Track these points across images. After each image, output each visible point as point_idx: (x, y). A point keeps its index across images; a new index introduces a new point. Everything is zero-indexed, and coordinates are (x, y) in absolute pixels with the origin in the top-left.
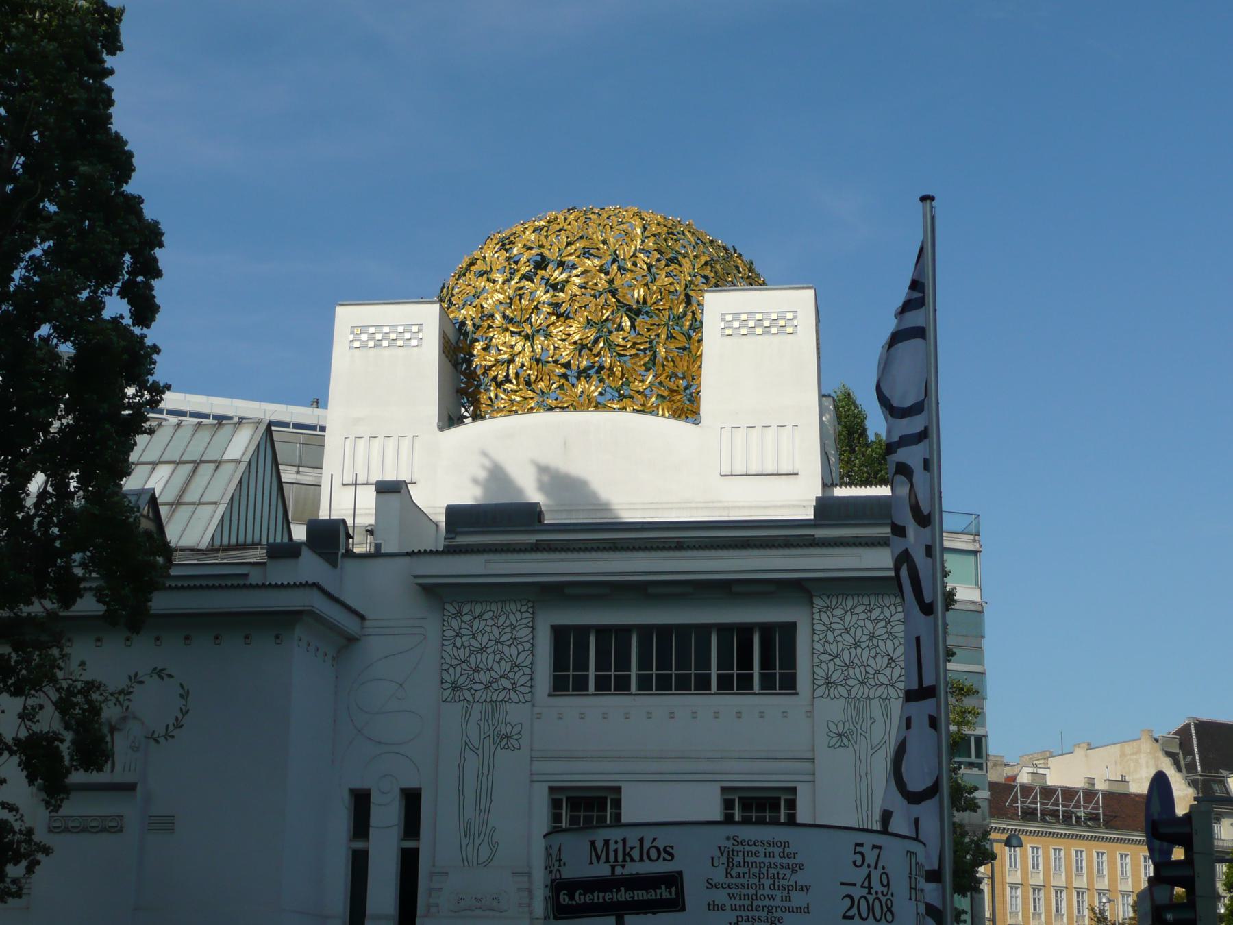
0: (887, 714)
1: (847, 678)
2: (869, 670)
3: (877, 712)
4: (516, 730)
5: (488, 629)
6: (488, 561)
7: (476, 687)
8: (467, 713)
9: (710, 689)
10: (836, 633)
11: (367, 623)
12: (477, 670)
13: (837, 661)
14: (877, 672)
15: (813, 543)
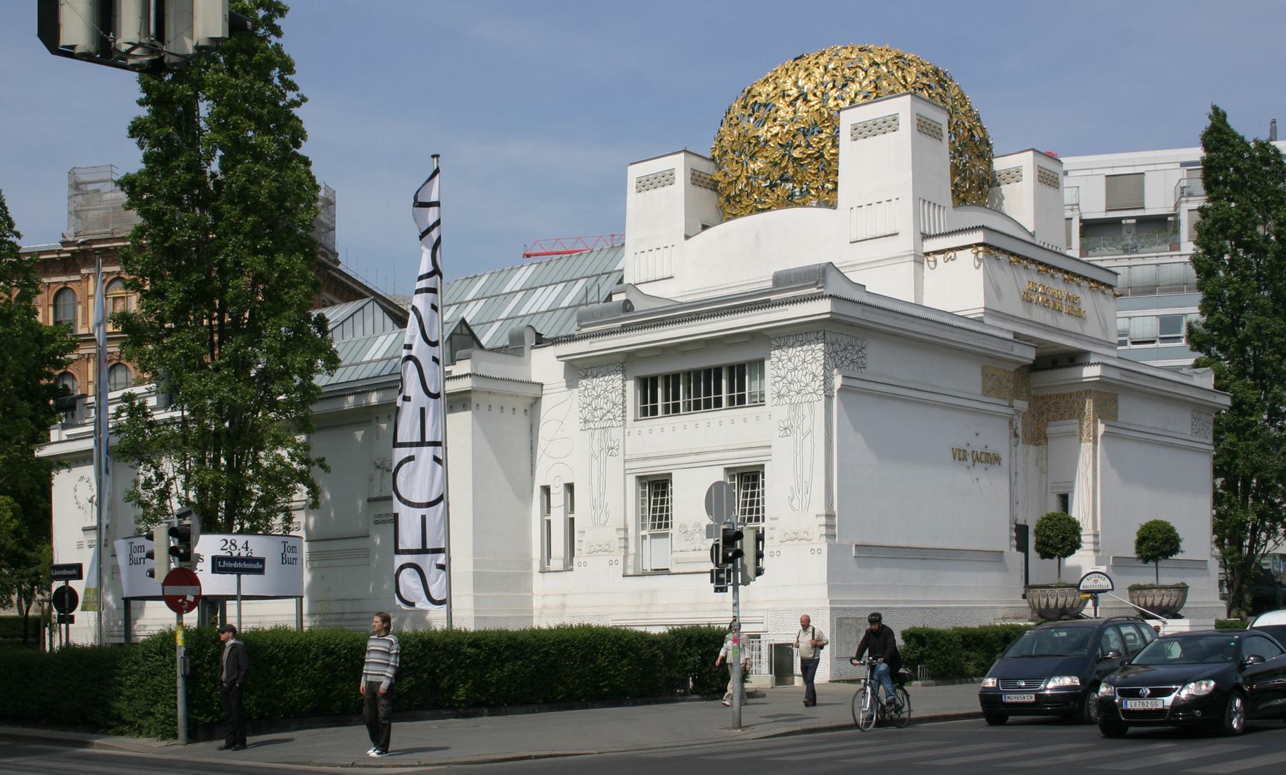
0: (812, 412)
1: (790, 391)
2: (803, 384)
3: (806, 412)
4: (617, 442)
5: (600, 383)
6: (591, 343)
7: (596, 419)
8: (592, 435)
9: (657, 414)
10: (784, 362)
11: (544, 387)
12: (595, 409)
13: (785, 381)
14: (807, 385)
15: (767, 304)
